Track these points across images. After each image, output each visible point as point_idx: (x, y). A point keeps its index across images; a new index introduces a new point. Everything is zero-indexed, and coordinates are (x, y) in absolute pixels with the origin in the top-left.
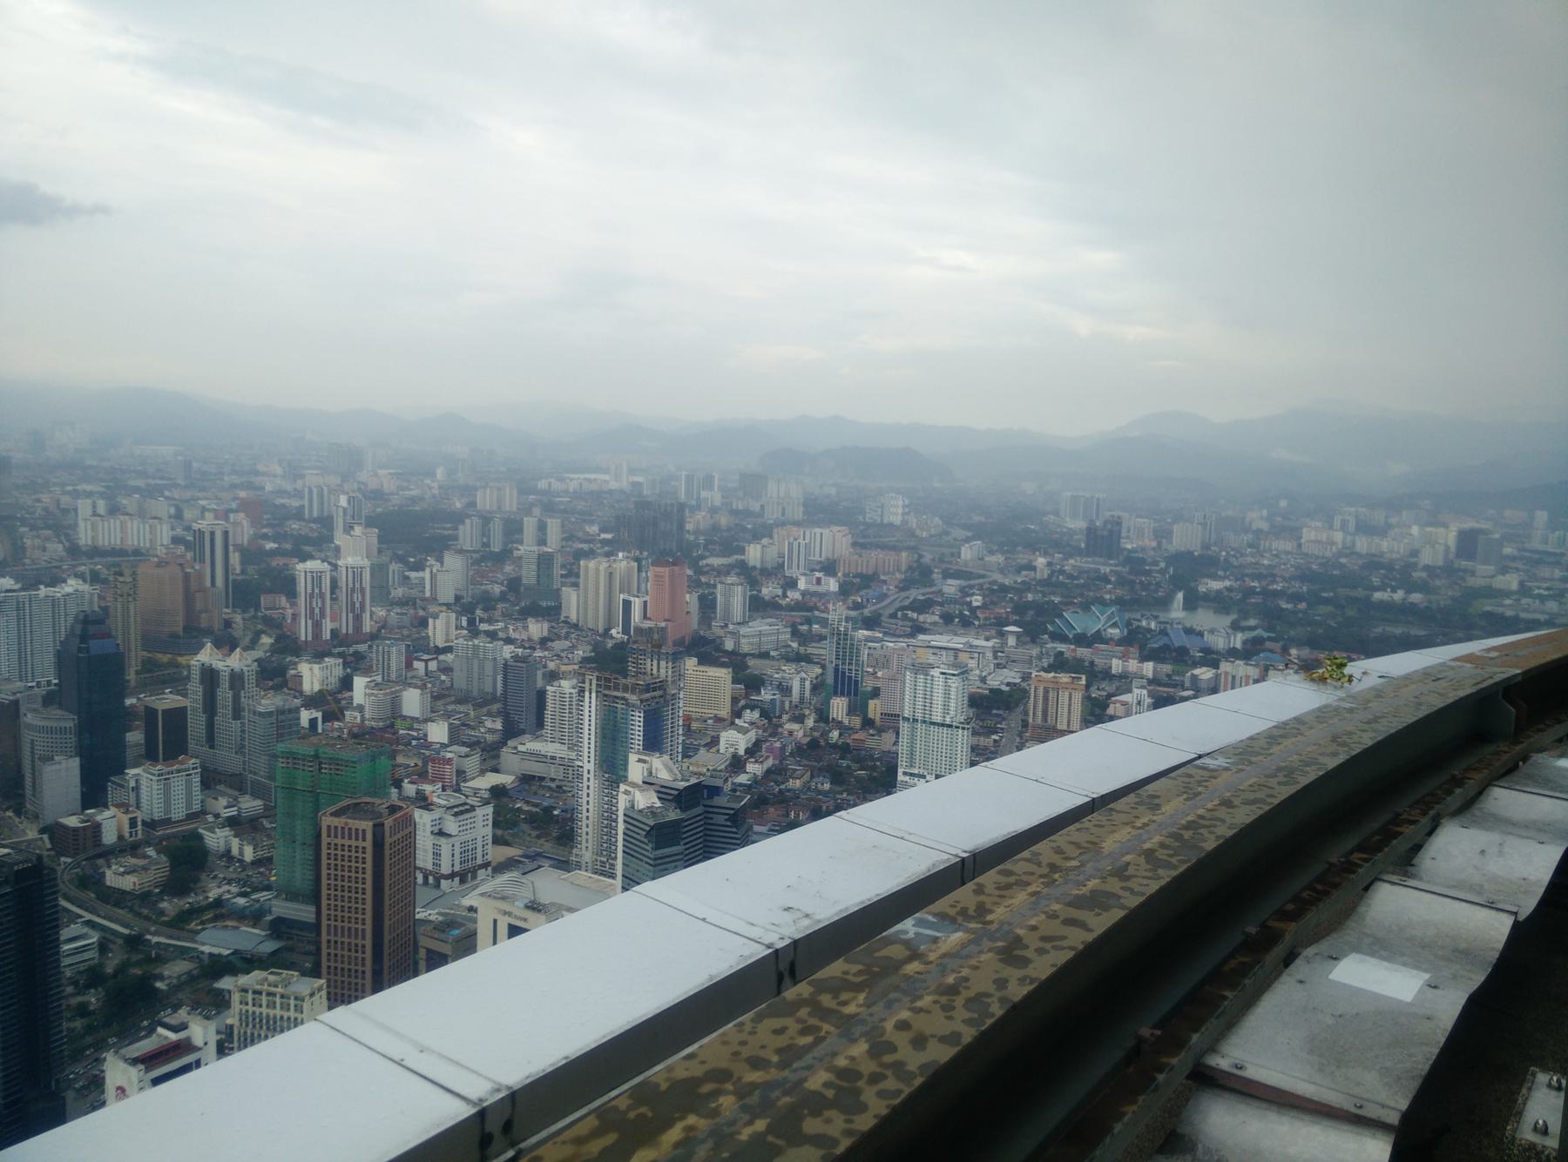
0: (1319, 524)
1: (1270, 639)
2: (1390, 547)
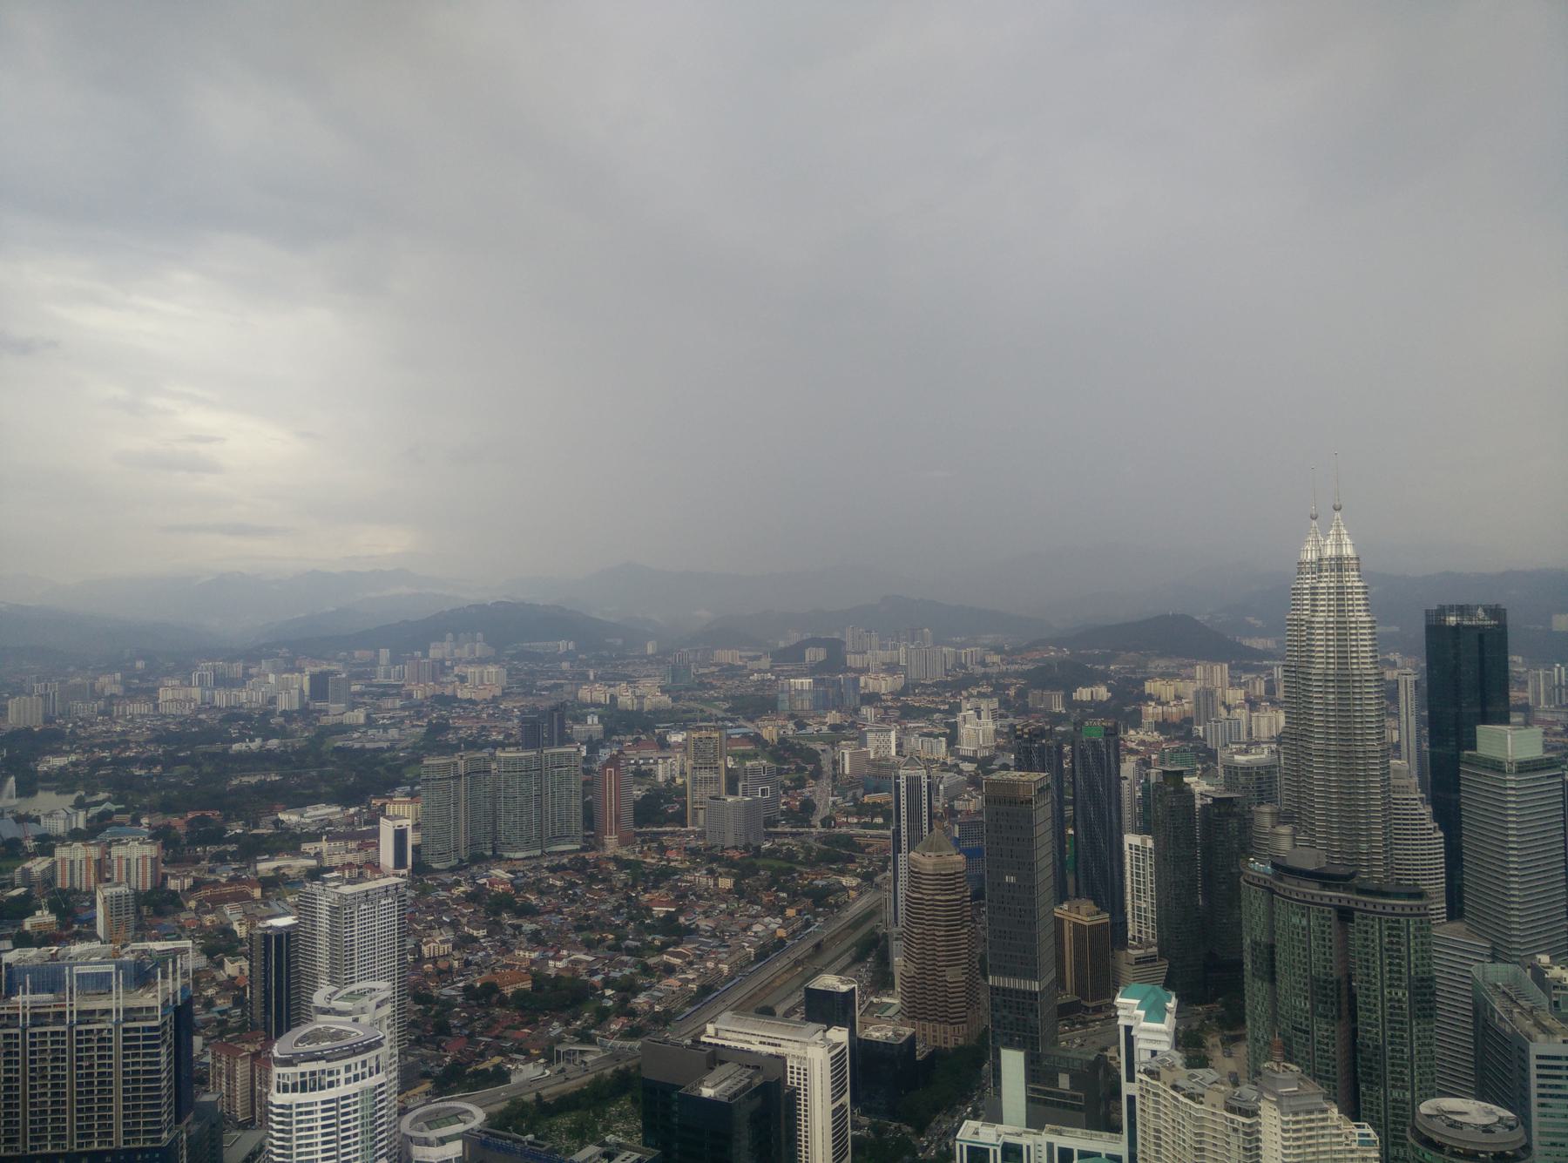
0: (176, 682)
1: (118, 812)
2: (248, 697)
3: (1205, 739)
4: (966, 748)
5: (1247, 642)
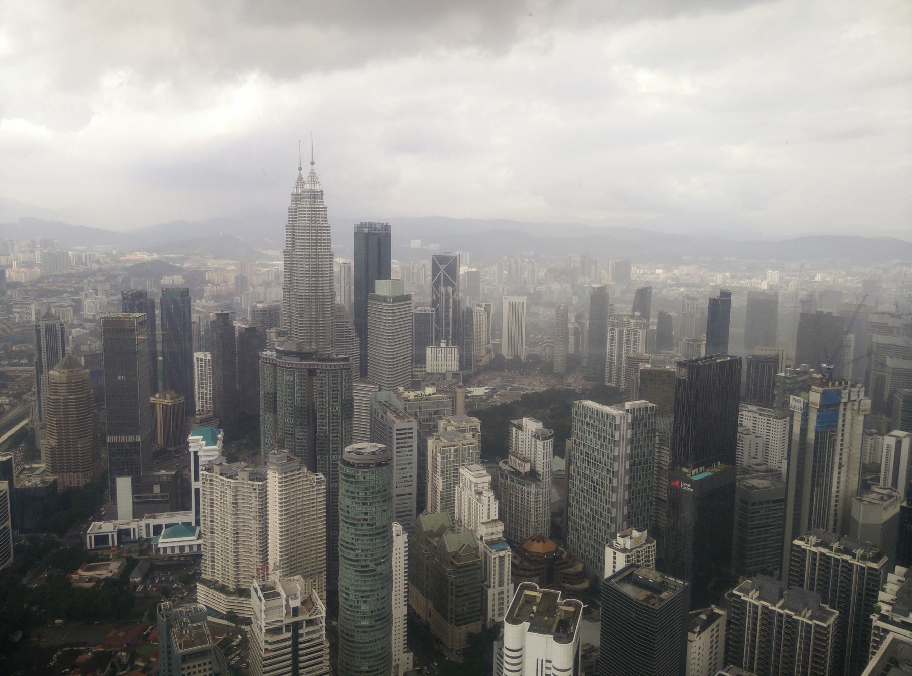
3: (241, 304)
4: (88, 313)
5: (264, 252)
